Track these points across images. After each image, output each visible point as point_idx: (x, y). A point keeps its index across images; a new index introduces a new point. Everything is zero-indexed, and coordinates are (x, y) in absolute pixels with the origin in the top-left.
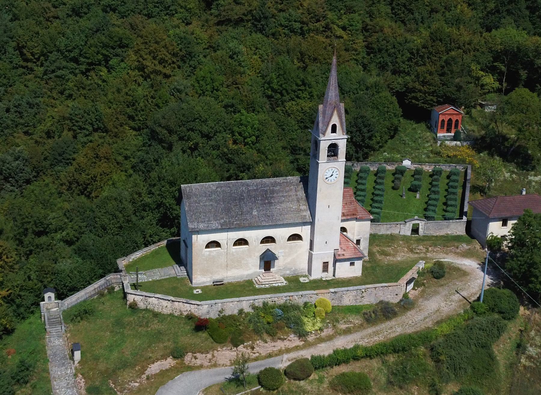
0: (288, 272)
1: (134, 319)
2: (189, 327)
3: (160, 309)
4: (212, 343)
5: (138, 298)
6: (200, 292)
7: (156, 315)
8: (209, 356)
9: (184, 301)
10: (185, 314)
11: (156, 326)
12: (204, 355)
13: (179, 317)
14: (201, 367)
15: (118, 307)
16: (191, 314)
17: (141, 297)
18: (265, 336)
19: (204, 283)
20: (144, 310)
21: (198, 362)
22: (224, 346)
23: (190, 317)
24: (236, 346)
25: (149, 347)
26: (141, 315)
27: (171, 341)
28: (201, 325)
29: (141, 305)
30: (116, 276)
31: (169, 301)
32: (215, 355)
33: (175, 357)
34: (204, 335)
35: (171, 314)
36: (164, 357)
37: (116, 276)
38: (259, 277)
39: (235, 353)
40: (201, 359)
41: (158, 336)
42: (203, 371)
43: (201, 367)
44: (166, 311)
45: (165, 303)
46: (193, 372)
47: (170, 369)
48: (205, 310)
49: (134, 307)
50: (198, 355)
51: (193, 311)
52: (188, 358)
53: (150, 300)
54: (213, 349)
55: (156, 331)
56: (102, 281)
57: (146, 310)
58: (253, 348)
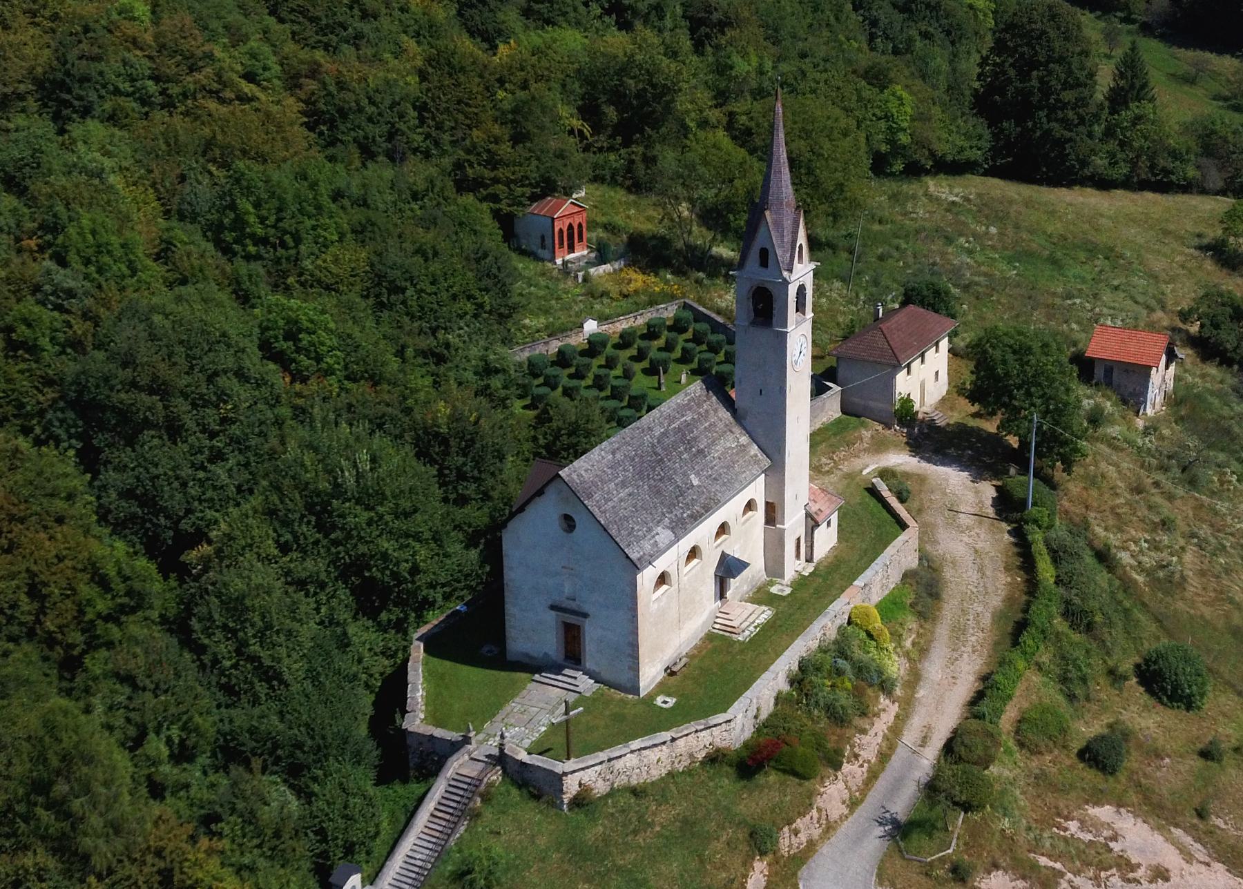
0: (745, 588)
1: (605, 827)
2: (727, 782)
3: (644, 773)
4: (800, 785)
5: (588, 776)
7: (636, 792)
8: (814, 812)
9: (699, 728)
10: (700, 756)
11: (663, 816)
12: (808, 817)
13: (689, 772)
14: (811, 845)
15: (539, 824)
16: (718, 750)
17: (598, 768)
18: (857, 721)
19: (655, 677)
20: (608, 795)
21: (803, 837)
22: (822, 778)
23: (715, 758)
24: (837, 766)
25: (702, 862)
26: (611, 810)
27: (727, 824)
29: (601, 788)
30: (461, 761)
31: (664, 743)
32: (821, 805)
33: (763, 854)
36: (747, 864)
37: (461, 761)
38: (719, 620)
39: (841, 785)
40: (807, 827)
41: (689, 831)
42: (825, 849)
43: (811, 845)
44: (657, 773)
45: (652, 755)
46: (812, 863)
47: (768, 882)
48: (736, 725)
49: (582, 801)
50: (799, 823)
51: (719, 743)
52: (787, 843)
53: (618, 765)
54: (811, 795)
55: (678, 824)
56: (439, 788)
57: (612, 793)
58: (856, 756)
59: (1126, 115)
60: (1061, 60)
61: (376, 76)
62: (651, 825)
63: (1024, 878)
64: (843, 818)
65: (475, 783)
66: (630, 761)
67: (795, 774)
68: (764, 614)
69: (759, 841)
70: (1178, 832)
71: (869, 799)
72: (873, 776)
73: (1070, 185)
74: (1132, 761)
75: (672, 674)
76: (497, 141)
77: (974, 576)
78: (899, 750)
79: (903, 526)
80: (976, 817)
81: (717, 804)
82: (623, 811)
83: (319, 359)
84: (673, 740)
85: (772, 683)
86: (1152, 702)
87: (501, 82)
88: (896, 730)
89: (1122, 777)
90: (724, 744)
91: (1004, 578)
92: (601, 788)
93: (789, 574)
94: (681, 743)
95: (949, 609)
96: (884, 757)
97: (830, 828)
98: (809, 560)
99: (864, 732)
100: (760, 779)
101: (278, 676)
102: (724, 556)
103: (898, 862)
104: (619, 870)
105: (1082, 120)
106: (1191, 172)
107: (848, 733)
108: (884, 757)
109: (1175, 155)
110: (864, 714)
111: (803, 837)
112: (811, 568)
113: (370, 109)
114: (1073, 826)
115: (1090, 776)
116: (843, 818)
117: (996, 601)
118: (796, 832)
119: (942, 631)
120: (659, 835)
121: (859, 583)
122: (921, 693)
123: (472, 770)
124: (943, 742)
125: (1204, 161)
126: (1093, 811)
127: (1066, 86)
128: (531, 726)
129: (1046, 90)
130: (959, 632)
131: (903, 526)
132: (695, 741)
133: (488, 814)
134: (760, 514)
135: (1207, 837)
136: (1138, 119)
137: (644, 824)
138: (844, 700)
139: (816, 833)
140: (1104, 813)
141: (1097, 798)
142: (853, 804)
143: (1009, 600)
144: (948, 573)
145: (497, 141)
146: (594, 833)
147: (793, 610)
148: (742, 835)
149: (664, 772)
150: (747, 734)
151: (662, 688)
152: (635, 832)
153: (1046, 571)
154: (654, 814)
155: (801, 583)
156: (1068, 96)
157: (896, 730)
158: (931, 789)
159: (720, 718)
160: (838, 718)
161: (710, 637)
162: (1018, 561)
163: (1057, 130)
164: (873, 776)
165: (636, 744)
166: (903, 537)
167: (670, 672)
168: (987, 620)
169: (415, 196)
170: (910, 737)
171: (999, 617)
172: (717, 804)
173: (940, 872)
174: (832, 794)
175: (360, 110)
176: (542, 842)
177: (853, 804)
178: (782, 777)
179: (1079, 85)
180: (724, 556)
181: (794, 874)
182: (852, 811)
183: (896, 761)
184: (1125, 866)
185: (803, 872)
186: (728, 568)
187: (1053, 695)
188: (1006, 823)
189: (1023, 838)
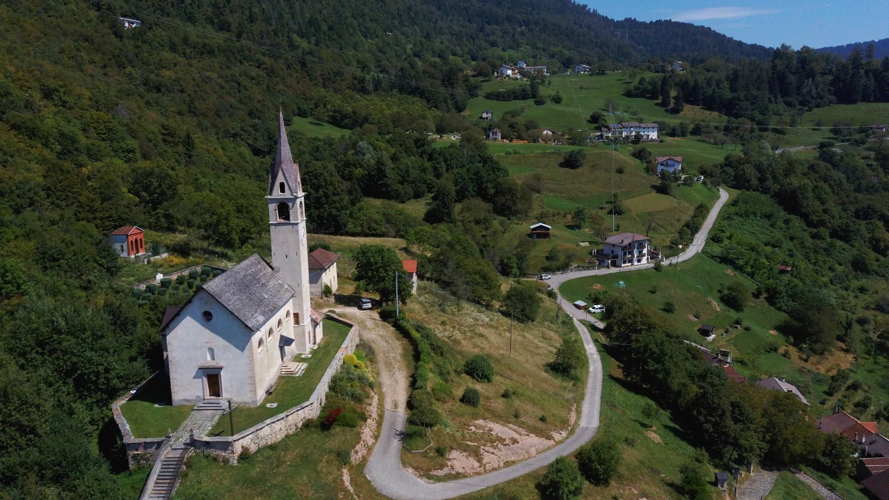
2: (316, 436)
5: (246, 442)
6: (275, 405)
7: (272, 447)
10: (300, 425)
13: (296, 434)
14: (365, 459)
15: (223, 473)
16: (309, 420)
17: (250, 436)
21: (360, 455)
23: (308, 425)
28: (328, 421)
29: (253, 448)
34: (337, 429)
35: (286, 436)
41: (306, 460)
42: (371, 459)
44: (280, 436)
45: (277, 426)
49: (245, 456)
50: (358, 447)
51: (308, 417)
52: (355, 458)
53: (261, 433)
54: (359, 434)
56: (157, 468)
57: (258, 451)
59: (356, 208)
60: (331, 184)
61: (18, 177)
62: (284, 462)
63: (465, 451)
64: (374, 444)
65: (180, 461)
66: (266, 431)
67: (349, 426)
68: (304, 366)
69: (342, 457)
70: (511, 425)
71: (382, 435)
72: (379, 424)
73: (342, 235)
74: (482, 402)
75: (270, 393)
76: (93, 201)
77: (385, 345)
78: (386, 412)
79: (351, 326)
80: (436, 428)
81: (315, 446)
82: (268, 458)
83: (19, 287)
84: (287, 416)
85: (322, 389)
86: (475, 381)
87: (89, 179)
88: (381, 405)
89: (480, 407)
90: (310, 417)
91: (398, 343)
92: (253, 448)
93: (308, 350)
94: (290, 418)
95: (380, 357)
96: (381, 416)
97: (370, 449)
98: (315, 343)
99: (370, 405)
100: (333, 431)
101: (33, 430)
102: (282, 337)
103: (409, 455)
104: (275, 486)
105: (342, 208)
106: (384, 230)
107: (364, 406)
108: (381, 416)
109: (376, 223)
110: (368, 397)
111: (360, 455)
112: (316, 347)
113: (17, 192)
114: (473, 428)
115: (468, 409)
116: (374, 444)
117: (399, 351)
118: (357, 452)
119: (381, 366)
120: (290, 466)
121: (343, 346)
122: (384, 390)
123: (177, 454)
124: (405, 405)
125: (387, 225)
126: (477, 422)
127: (334, 194)
128: (202, 428)
129: (326, 196)
130: (389, 365)
131: (351, 326)
132: (297, 417)
133: (191, 474)
134: (292, 318)
135: (522, 425)
136: (360, 209)
137: (280, 463)
138: (358, 391)
139: (365, 452)
140: (480, 422)
141: (475, 417)
142: (376, 437)
143: (404, 349)
144: (373, 345)
145: (93, 201)
146: (254, 472)
147: (320, 357)
148: (333, 457)
149: (283, 436)
150: (318, 413)
151: (266, 401)
152: (278, 467)
153: (416, 335)
154: (284, 456)
155: (314, 352)
156: (336, 198)
157: (381, 405)
158: (410, 421)
159: (307, 403)
160: (358, 399)
161: (281, 378)
162: (401, 335)
163: (334, 212)
164: (379, 424)
165: (268, 421)
166: (353, 329)
167: (269, 393)
168: (399, 358)
169: (53, 223)
170: (388, 406)
171: (404, 356)
172: (315, 446)
173: (432, 454)
174: (367, 432)
175: (12, 192)
176: (226, 482)
177: (376, 437)
178: (342, 428)
179: (338, 194)
180: (282, 337)
181: (362, 473)
182: (376, 440)
183: (387, 415)
184: (502, 440)
185: (366, 471)
186: (285, 342)
187: (438, 380)
188: (448, 430)
189: (458, 435)
